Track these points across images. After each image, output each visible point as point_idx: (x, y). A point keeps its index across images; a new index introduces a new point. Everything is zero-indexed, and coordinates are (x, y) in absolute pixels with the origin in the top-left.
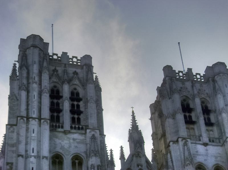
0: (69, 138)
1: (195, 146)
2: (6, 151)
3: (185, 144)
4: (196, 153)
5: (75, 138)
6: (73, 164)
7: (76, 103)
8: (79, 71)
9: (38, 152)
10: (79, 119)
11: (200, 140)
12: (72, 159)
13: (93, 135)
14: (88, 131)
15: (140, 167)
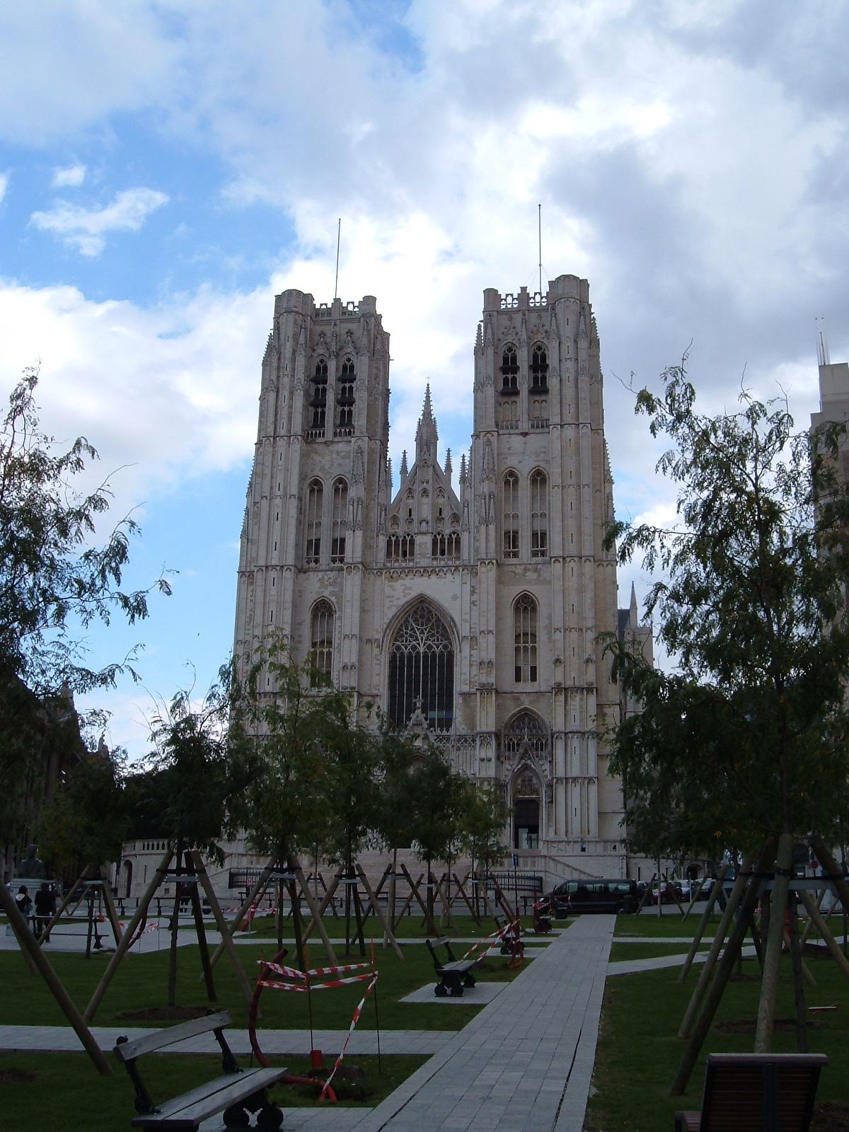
0: (331, 452)
1: (509, 438)
2: (253, 486)
3: (489, 443)
4: (507, 451)
5: (339, 450)
6: (337, 490)
7: (347, 385)
8: (353, 326)
9: (285, 488)
10: (350, 412)
11: (517, 428)
12: (335, 483)
13: (360, 447)
14: (353, 440)
15: (425, 484)
